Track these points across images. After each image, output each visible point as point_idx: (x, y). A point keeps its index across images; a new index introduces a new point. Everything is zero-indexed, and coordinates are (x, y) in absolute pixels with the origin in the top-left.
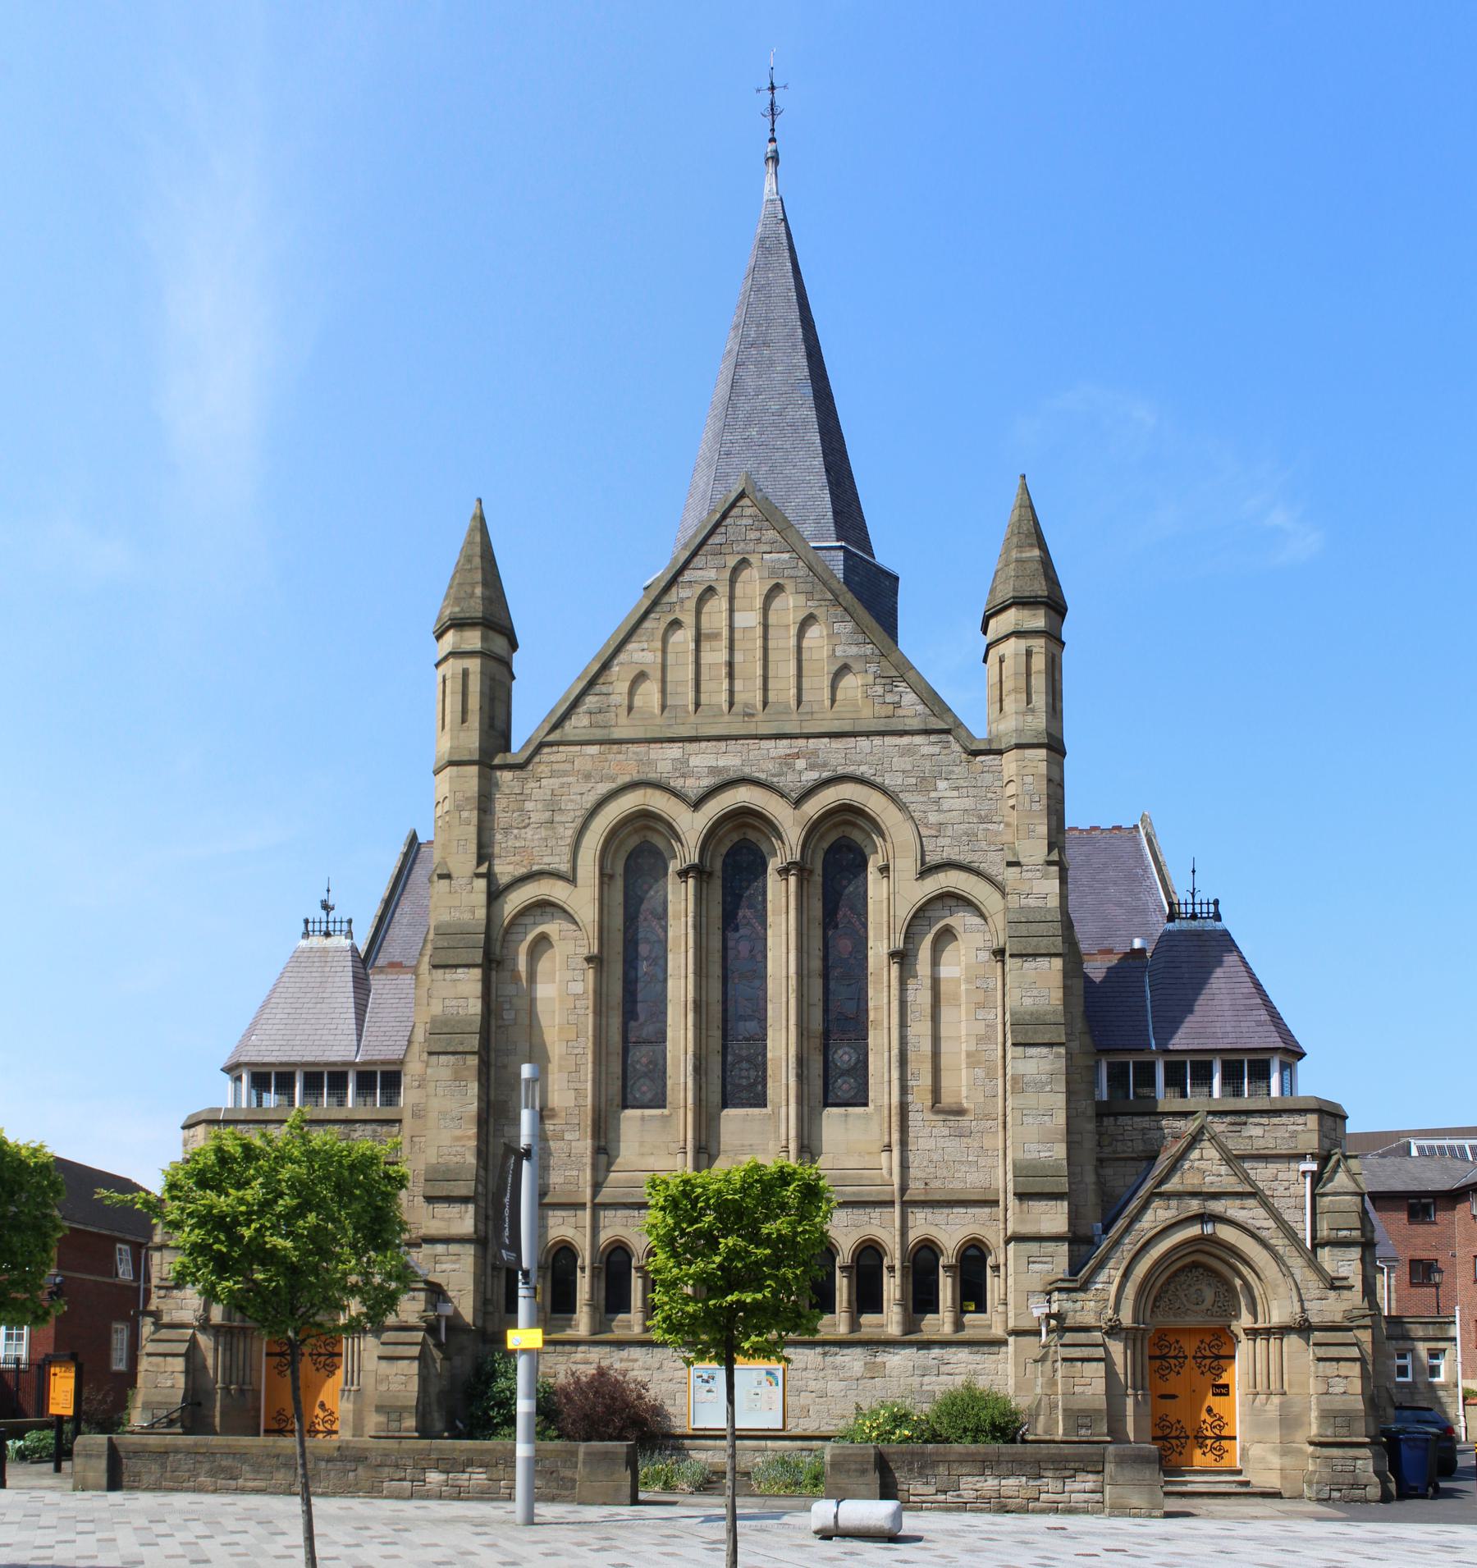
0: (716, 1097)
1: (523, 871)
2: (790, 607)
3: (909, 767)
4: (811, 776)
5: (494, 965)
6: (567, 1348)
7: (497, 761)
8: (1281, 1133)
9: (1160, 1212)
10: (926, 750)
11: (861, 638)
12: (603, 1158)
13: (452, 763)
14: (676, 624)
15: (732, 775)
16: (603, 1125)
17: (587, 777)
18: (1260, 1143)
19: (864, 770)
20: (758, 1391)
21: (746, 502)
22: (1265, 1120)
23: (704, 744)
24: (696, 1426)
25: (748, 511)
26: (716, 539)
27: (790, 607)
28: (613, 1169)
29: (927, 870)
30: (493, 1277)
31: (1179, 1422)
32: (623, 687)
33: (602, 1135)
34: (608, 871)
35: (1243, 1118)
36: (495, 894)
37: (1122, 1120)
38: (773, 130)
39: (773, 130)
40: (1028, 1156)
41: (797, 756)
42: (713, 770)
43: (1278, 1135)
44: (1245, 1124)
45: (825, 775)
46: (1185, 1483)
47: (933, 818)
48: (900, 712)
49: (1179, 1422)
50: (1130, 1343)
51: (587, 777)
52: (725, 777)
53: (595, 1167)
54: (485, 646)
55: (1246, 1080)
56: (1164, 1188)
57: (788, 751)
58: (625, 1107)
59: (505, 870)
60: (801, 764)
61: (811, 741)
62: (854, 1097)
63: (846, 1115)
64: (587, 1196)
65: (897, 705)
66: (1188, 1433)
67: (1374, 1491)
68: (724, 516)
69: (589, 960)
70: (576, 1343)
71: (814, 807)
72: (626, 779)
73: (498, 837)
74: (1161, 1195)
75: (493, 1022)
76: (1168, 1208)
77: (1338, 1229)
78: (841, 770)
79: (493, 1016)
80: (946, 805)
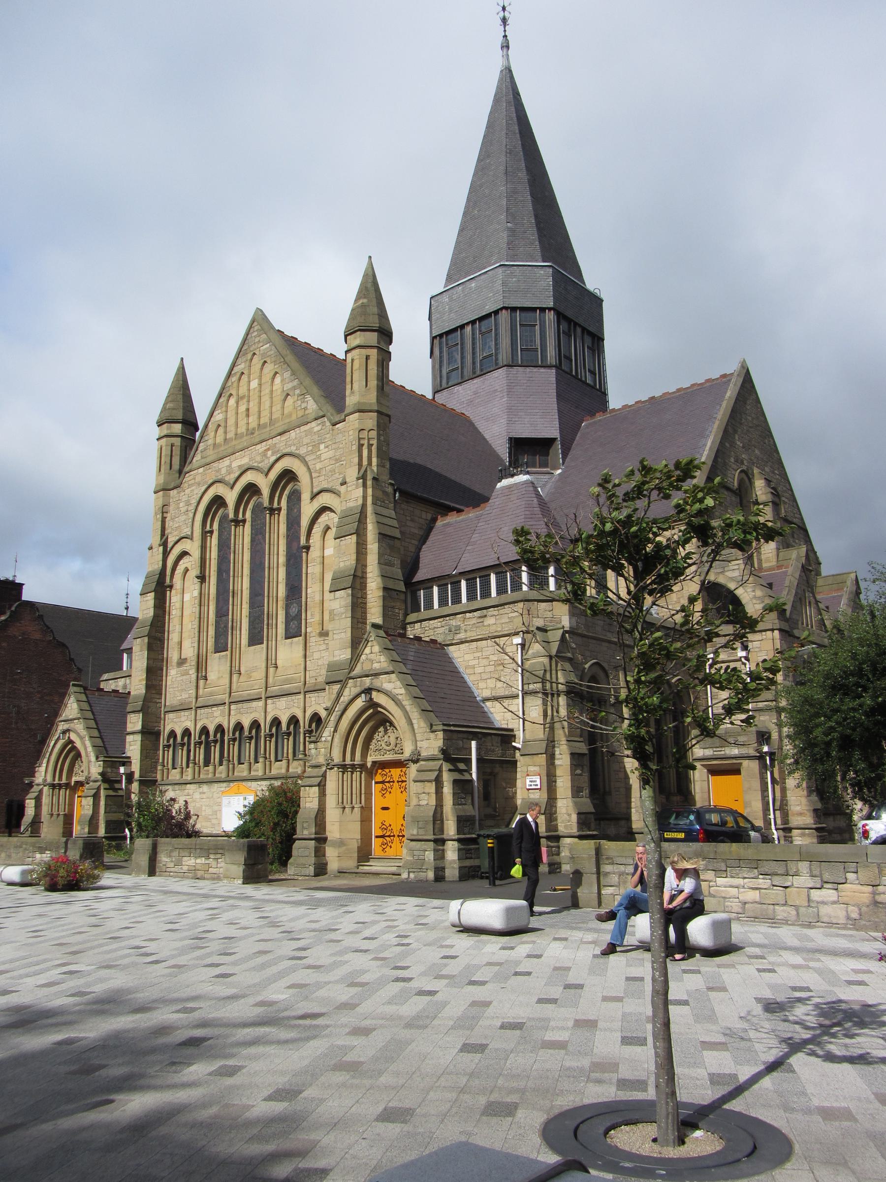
1: (177, 538)
2: (269, 368)
3: (309, 441)
4: (273, 458)
10: (316, 429)
11: (292, 378)
13: (164, 490)
14: (231, 395)
15: (246, 467)
17: (199, 484)
19: (293, 449)
21: (255, 324)
25: (256, 328)
26: (245, 347)
27: (269, 368)
29: (314, 497)
32: (212, 434)
36: (166, 554)
40: (335, 659)
41: (268, 449)
42: (240, 466)
45: (278, 455)
47: (318, 466)
48: (307, 412)
51: (199, 484)
52: (244, 469)
57: (265, 448)
59: (171, 540)
60: (269, 453)
62: (296, 632)
63: (292, 643)
65: (305, 409)
68: (248, 335)
69: (198, 577)
71: (273, 475)
72: (211, 481)
78: (285, 451)
80: (323, 457)
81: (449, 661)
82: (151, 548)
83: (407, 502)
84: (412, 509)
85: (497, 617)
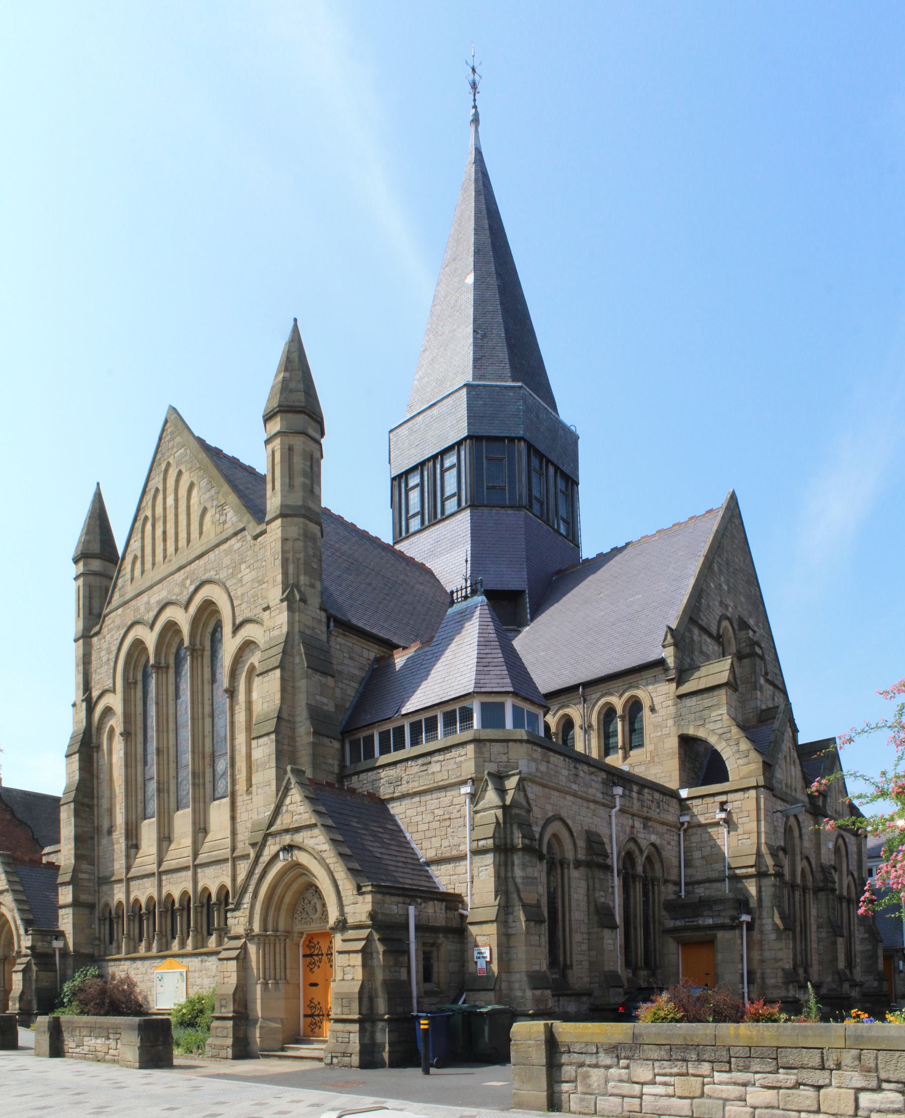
0: (173, 805)
5: (95, 749)
6: (118, 963)
7: (92, 633)
8: (451, 765)
9: (272, 847)
12: (133, 851)
16: (134, 832)
18: (439, 777)
20: (178, 985)
22: (441, 758)
23: (155, 588)
24: (158, 1008)
26: (158, 457)
28: (138, 856)
30: (100, 925)
31: (319, 1003)
33: (134, 837)
34: (131, 680)
35: (428, 759)
37: (363, 776)
38: (475, 100)
39: (475, 100)
43: (450, 767)
44: (430, 763)
46: (298, 1049)
49: (319, 1003)
50: (261, 946)
52: (162, 604)
53: (128, 857)
54: (86, 569)
55: (458, 724)
56: (273, 829)
58: (145, 819)
61: (192, 565)
64: (123, 876)
66: (324, 1012)
67: (355, 1060)
70: (120, 960)
72: (130, 623)
73: (94, 676)
74: (270, 834)
75: (95, 781)
76: (275, 844)
77: (478, 840)
79: (95, 778)
81: (392, 819)
82: (74, 705)
83: (344, 635)
84: (350, 644)
85: (443, 763)
